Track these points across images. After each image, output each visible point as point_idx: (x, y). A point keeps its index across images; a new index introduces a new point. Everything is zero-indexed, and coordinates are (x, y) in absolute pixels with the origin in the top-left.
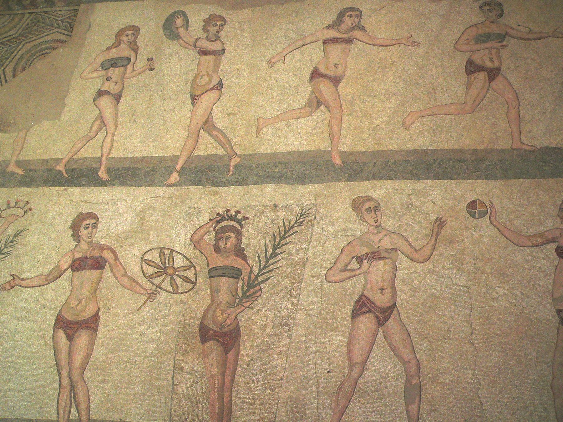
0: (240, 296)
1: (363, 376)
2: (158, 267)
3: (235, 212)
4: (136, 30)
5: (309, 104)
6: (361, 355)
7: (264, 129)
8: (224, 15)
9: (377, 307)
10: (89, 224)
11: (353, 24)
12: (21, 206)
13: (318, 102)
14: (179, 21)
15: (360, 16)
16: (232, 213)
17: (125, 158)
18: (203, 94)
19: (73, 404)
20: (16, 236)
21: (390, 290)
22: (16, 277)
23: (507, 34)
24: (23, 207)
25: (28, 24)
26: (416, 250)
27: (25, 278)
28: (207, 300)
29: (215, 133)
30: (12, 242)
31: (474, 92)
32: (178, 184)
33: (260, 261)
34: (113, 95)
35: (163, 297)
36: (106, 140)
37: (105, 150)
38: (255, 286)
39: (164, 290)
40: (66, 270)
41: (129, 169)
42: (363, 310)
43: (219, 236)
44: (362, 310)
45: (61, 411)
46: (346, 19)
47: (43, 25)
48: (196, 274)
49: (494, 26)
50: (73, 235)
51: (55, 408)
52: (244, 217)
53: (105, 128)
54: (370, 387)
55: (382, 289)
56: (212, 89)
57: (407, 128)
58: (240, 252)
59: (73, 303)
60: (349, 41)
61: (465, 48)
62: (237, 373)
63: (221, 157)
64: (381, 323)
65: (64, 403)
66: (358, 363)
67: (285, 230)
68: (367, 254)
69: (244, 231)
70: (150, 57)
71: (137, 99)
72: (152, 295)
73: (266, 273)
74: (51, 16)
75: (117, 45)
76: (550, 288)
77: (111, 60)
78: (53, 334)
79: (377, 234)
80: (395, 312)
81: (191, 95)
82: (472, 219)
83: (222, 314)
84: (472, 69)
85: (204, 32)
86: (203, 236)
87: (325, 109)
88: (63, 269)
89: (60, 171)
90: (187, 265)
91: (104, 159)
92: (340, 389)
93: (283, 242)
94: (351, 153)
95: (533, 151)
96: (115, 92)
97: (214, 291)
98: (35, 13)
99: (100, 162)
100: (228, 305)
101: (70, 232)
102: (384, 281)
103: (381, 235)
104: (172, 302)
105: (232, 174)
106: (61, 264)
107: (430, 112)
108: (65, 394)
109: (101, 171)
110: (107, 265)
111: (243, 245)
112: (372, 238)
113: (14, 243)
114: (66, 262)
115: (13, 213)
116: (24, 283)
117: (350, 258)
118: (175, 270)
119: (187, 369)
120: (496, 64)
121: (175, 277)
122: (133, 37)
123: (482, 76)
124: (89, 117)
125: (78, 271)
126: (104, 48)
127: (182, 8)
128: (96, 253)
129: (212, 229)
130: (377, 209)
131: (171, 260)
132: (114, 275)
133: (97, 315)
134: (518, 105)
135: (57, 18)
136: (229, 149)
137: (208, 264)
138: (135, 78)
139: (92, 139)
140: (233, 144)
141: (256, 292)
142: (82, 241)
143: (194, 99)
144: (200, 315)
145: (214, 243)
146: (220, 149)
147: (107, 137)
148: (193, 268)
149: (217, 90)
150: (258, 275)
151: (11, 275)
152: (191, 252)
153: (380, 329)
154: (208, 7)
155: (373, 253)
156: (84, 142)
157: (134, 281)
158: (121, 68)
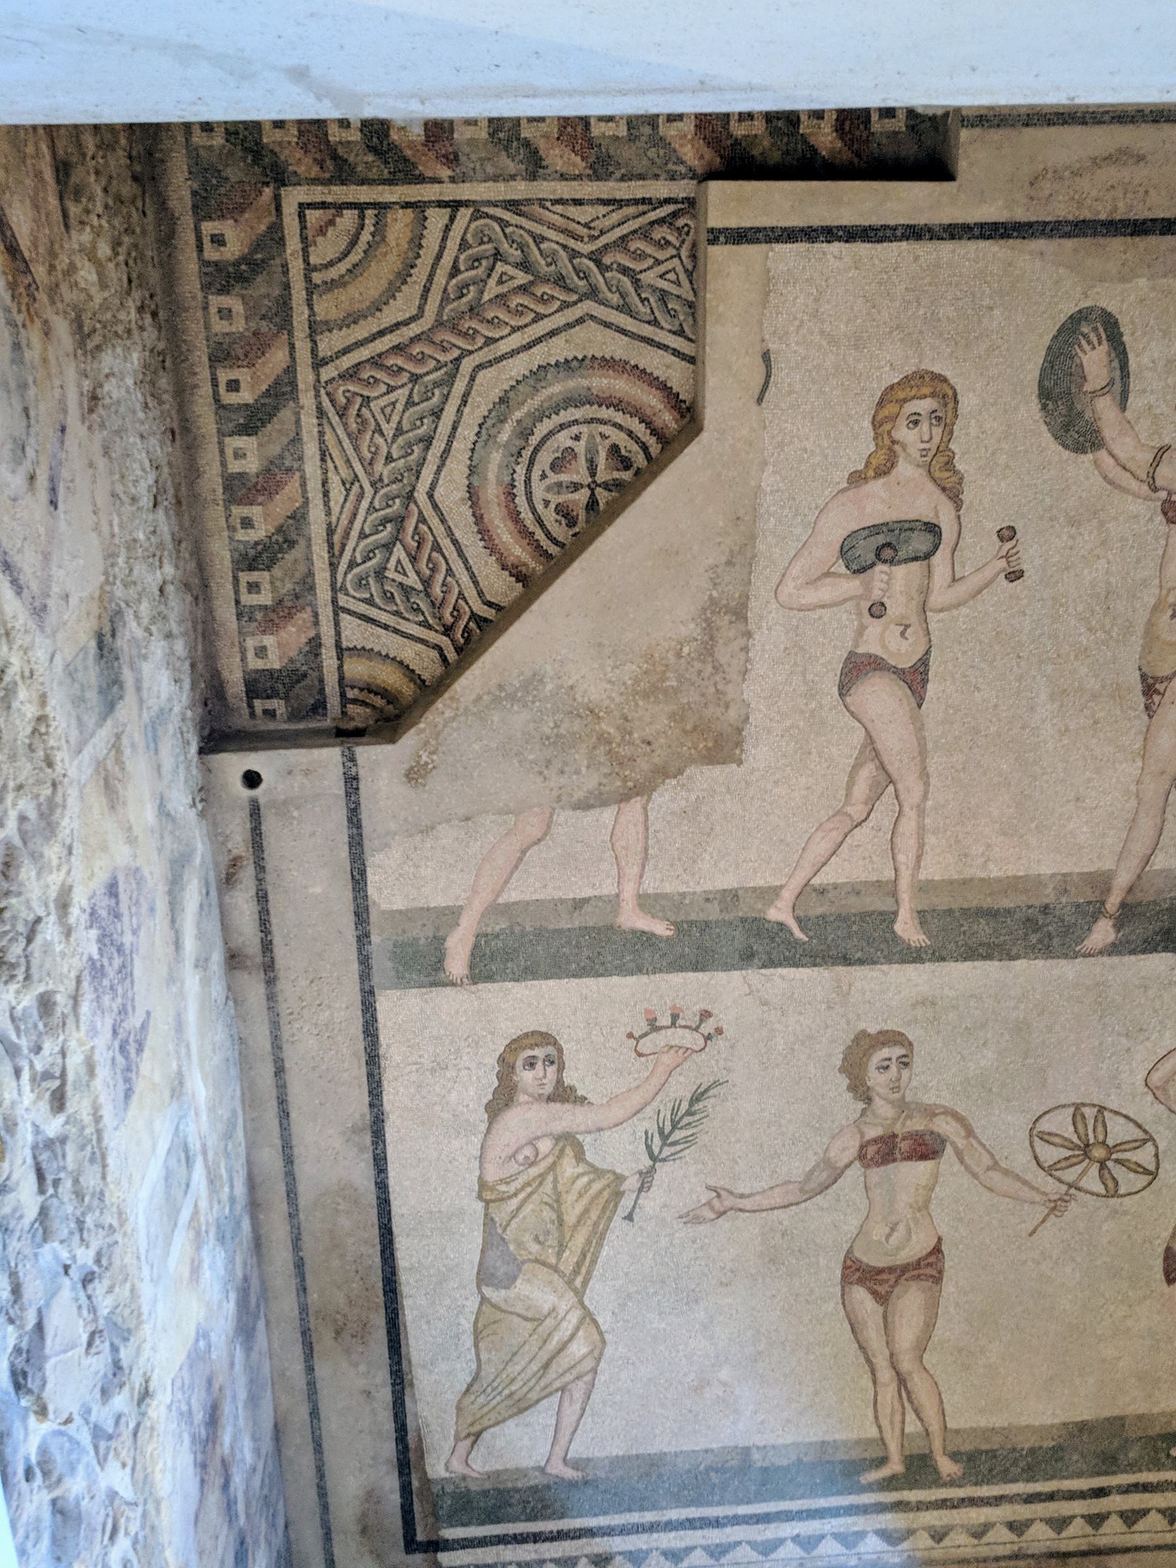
34: (899, 673)
40: (848, 1166)
71: (978, 689)
88: (841, 1164)
96: (905, 664)
101: (844, 1082)
106: (832, 1154)
109: (900, 918)
114: (846, 1148)
124: (834, 750)
125: (878, 1165)
138: (964, 610)
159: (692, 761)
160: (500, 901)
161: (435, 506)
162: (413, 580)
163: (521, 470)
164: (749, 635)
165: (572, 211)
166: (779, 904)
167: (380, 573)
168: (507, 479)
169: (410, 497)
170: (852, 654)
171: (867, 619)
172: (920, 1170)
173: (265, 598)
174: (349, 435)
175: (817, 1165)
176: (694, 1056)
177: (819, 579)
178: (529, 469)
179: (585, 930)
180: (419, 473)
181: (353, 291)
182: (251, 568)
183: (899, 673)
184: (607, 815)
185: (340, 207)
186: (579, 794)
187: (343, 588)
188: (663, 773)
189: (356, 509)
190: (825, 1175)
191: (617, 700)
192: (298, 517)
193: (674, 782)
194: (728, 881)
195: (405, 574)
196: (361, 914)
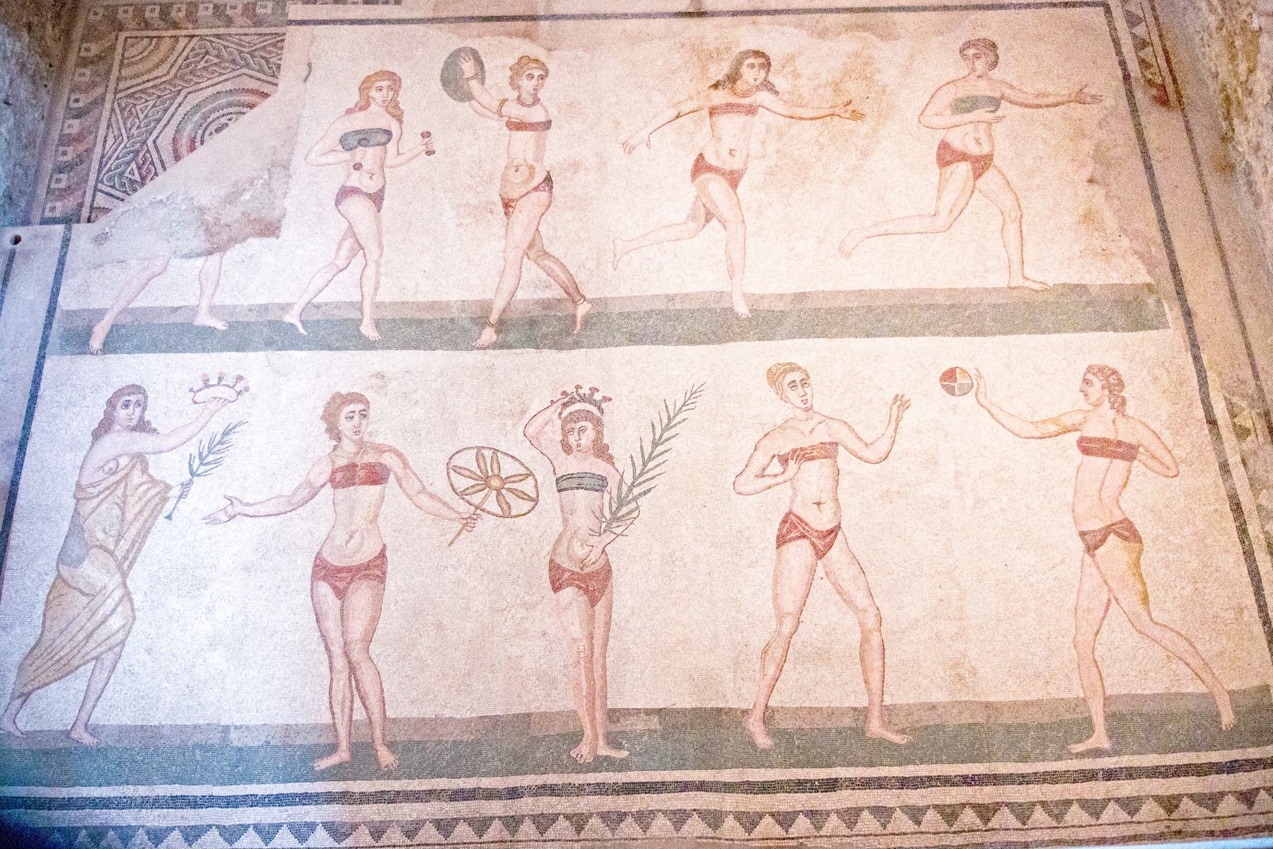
0: (608, 518)
1: (799, 631)
2: (475, 477)
3: (590, 389)
4: (395, 80)
5: (693, 218)
6: (794, 602)
7: (625, 258)
8: (543, 59)
9: (813, 529)
10: (354, 412)
11: (755, 80)
12: (229, 383)
13: (707, 214)
14: (468, 67)
15: (767, 65)
16: (585, 390)
17: (403, 303)
18: (523, 196)
19: (357, 699)
20: (225, 434)
21: (832, 505)
22: (235, 501)
23: (1003, 97)
24: (234, 386)
25: (187, 58)
26: (866, 444)
27: (252, 501)
28: (558, 526)
29: (548, 263)
30: (220, 443)
31: (950, 196)
32: (495, 346)
33: (633, 464)
34: (369, 196)
35: (486, 524)
36: (365, 273)
37: (368, 289)
38: (629, 502)
39: (489, 513)
40: (322, 486)
41: (411, 322)
42: (792, 535)
43: (569, 426)
44: (792, 535)
45: (337, 709)
46: (745, 70)
47: (216, 60)
48: (536, 486)
49: (982, 84)
50: (329, 430)
51: (328, 705)
52: (604, 397)
53: (362, 251)
54: (809, 649)
55: (818, 504)
56: (536, 189)
57: (848, 256)
58: (601, 451)
59: (341, 537)
60: (751, 110)
61: (936, 121)
62: (611, 634)
64: (820, 554)
65: (340, 698)
66: (789, 614)
67: (669, 417)
68: (794, 451)
69: (605, 419)
70: (426, 130)
72: (469, 520)
73: (644, 482)
74: (230, 45)
75: (364, 105)
76: (1070, 498)
78: (312, 589)
79: (807, 420)
80: (840, 536)
81: (503, 199)
82: (949, 396)
83: (582, 546)
84: (948, 158)
85: (514, 89)
86: (543, 428)
87: (719, 225)
89: (292, 324)
90: (520, 472)
92: (765, 652)
93: (666, 435)
94: (763, 297)
95: (1042, 291)
97: (567, 513)
98: (197, 36)
99: (361, 310)
100: (591, 533)
102: (822, 491)
103: (813, 423)
104: (502, 530)
105: (581, 329)
107: (882, 230)
108: (341, 683)
110: (392, 477)
111: (606, 441)
112: (800, 427)
113: (225, 446)
115: (217, 396)
116: (250, 511)
117: (768, 458)
118: (504, 481)
119: (535, 631)
120: (986, 149)
121: (504, 492)
122: (391, 94)
123: (963, 169)
126: (342, 110)
127: (470, 43)
128: (370, 458)
129: (556, 416)
130: (804, 383)
131: (495, 466)
132: (404, 491)
133: (382, 555)
134: (1019, 216)
135: (241, 48)
137: (554, 470)
141: (632, 511)
142: (344, 439)
143: (507, 205)
144: (548, 548)
145: (561, 438)
148: (531, 477)
149: (545, 190)
150: (633, 485)
151: (226, 497)
152: (527, 454)
153: (819, 562)
154: (516, 41)
155: (802, 449)
156: (329, 276)
157: (440, 501)
159: (251, 235)
160: (130, 306)
161: (156, 146)
162: (137, 177)
163: (200, 132)
164: (290, 176)
165: (244, 37)
166: (292, 313)
167: (121, 175)
168: (193, 135)
169: (145, 142)
170: (343, 186)
171: (352, 170)
172: (369, 493)
173: (62, 185)
174: (123, 119)
175: (301, 485)
176: (229, 404)
177: (328, 152)
178: (204, 131)
179: (175, 325)
180: (151, 133)
181: (140, 66)
182: (60, 172)
183: (369, 196)
184: (199, 262)
185: (142, 38)
186: (186, 251)
187: (102, 182)
188: (233, 241)
189: (118, 147)
190: (306, 491)
191: (216, 204)
192: (89, 151)
193: (239, 246)
194: (262, 299)
195: (134, 175)
196: (51, 312)
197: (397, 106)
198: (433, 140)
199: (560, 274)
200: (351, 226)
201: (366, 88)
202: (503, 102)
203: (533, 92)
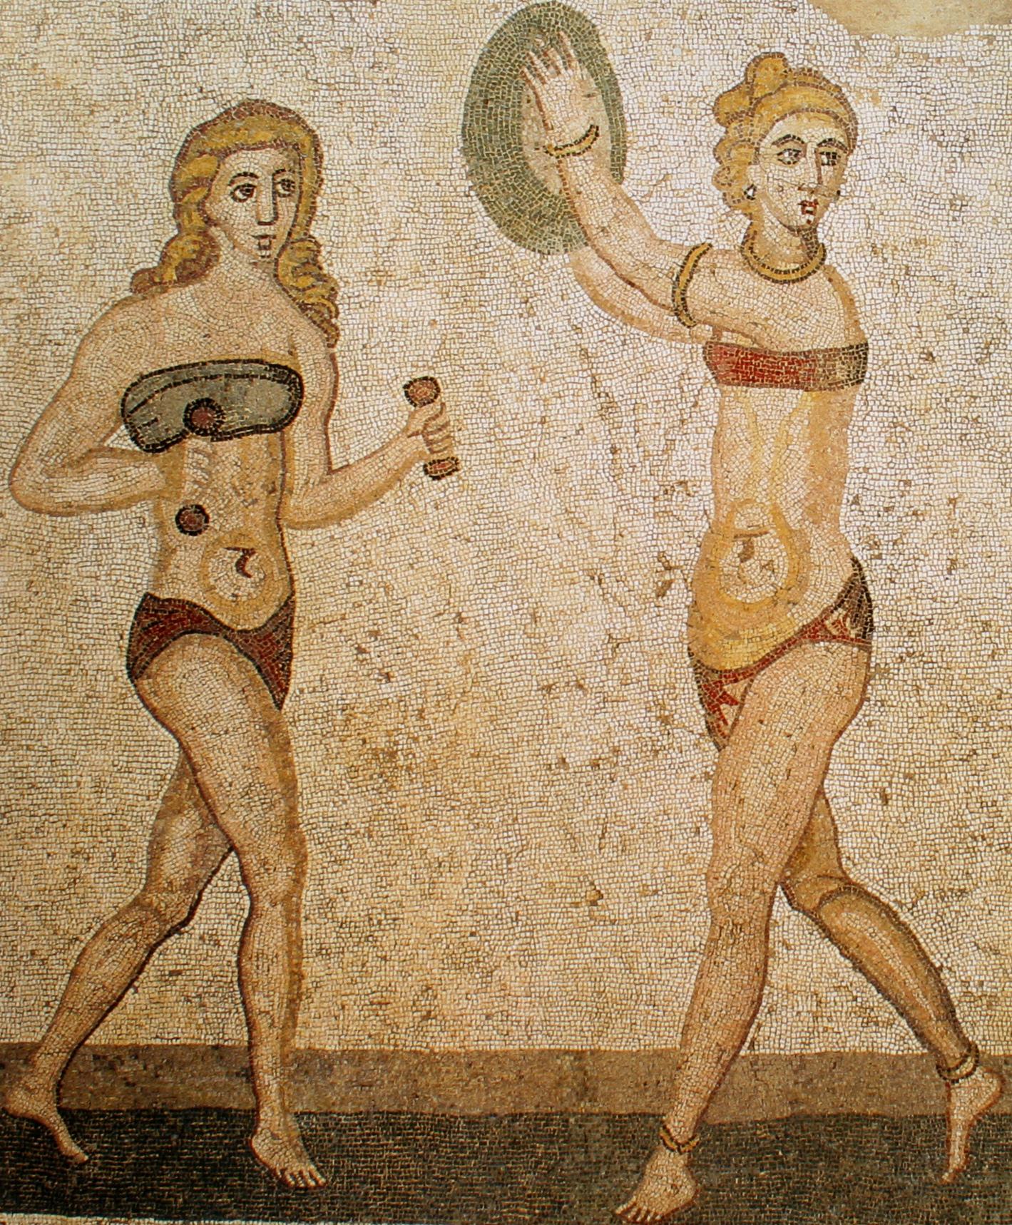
18: (765, 662)
29: (852, 920)
36: (255, 945)
56: (814, 632)
63: (897, 1064)
77: (178, 376)
81: (700, 669)
89: (37, 1126)
91: (266, 1056)
99: (250, 1074)
136: (936, 1029)
139: (176, 930)
140: (955, 993)
146: (889, 1024)
147: (260, 925)
149: (843, 638)
158: (257, 442)
170: (149, 598)
197: (311, 265)
198: (450, 416)
199: (896, 964)
200: (189, 766)
201: (199, 181)
202: (695, 257)
203: (803, 220)
